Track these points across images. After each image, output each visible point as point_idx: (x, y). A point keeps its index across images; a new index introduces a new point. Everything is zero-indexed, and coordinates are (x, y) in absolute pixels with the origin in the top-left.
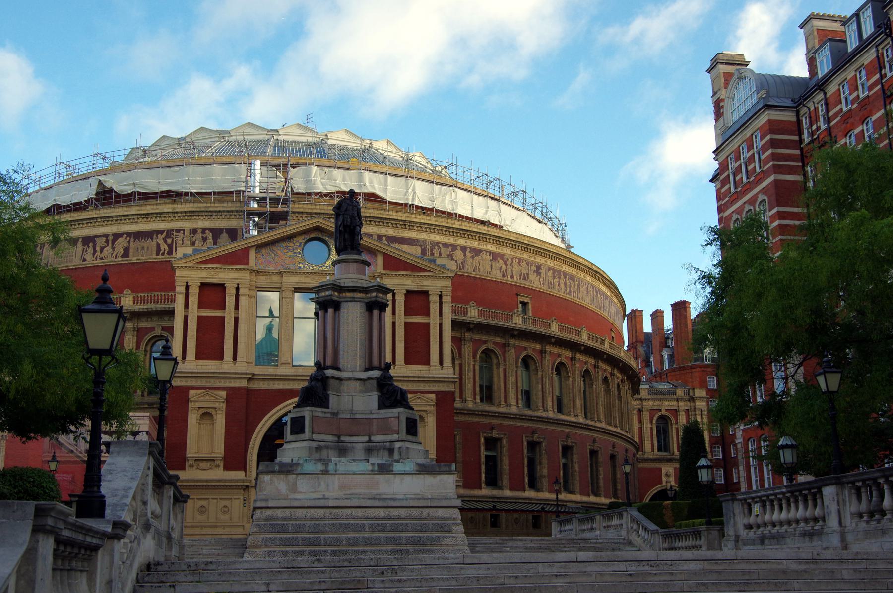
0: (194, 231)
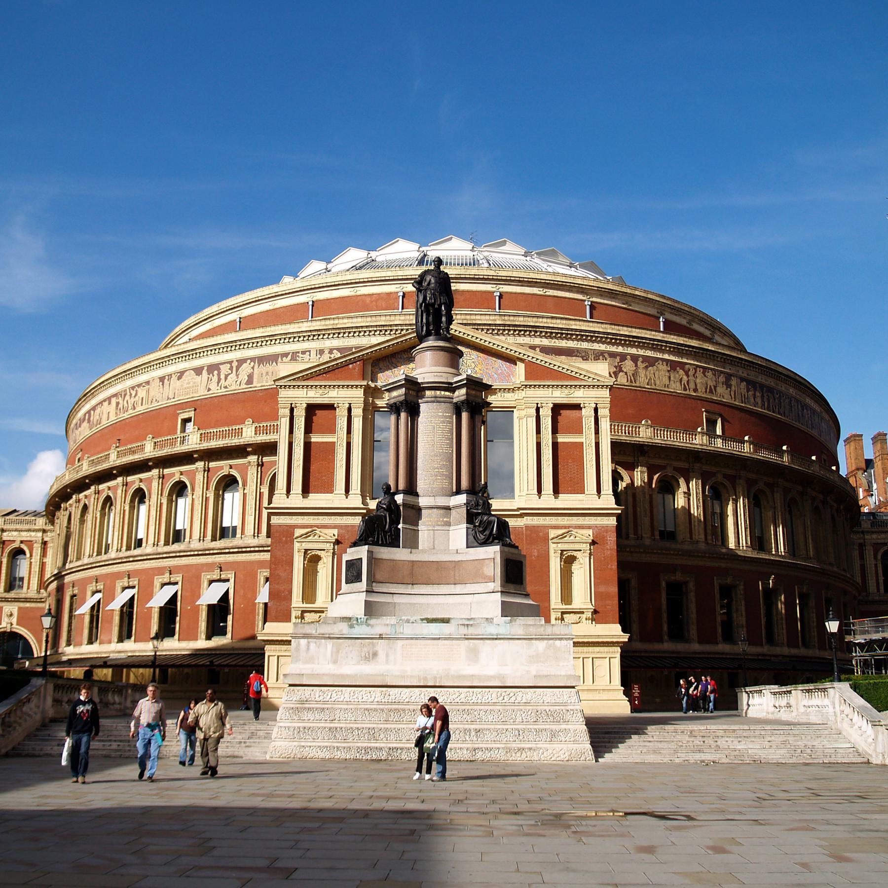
0: (321, 352)
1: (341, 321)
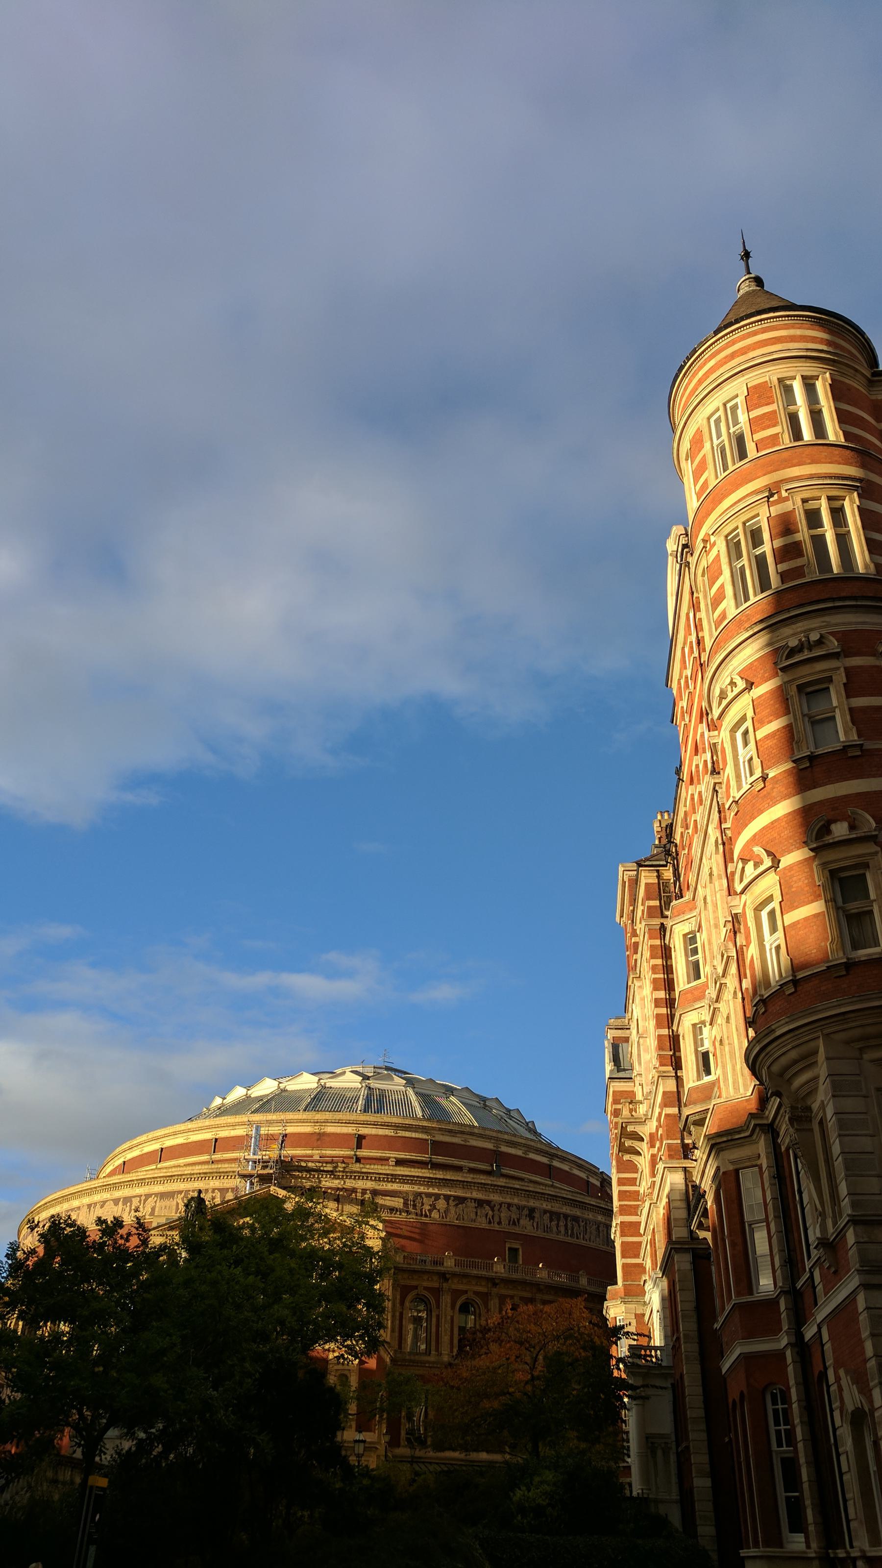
1: (223, 1166)
